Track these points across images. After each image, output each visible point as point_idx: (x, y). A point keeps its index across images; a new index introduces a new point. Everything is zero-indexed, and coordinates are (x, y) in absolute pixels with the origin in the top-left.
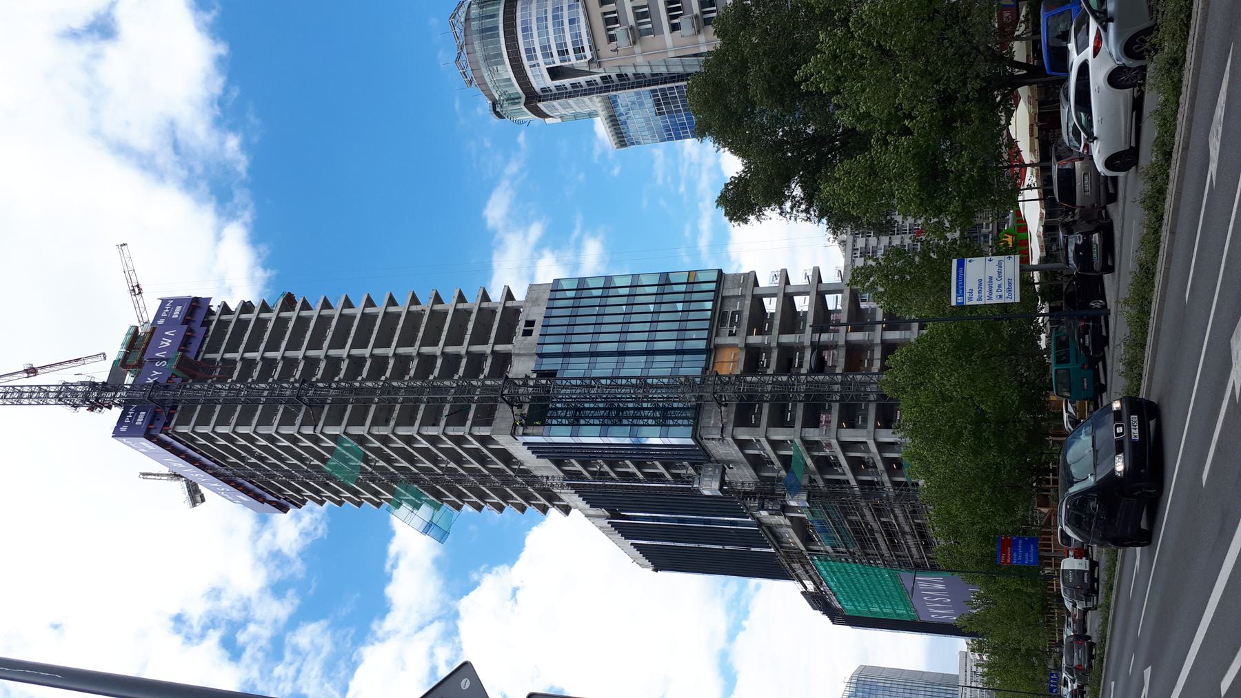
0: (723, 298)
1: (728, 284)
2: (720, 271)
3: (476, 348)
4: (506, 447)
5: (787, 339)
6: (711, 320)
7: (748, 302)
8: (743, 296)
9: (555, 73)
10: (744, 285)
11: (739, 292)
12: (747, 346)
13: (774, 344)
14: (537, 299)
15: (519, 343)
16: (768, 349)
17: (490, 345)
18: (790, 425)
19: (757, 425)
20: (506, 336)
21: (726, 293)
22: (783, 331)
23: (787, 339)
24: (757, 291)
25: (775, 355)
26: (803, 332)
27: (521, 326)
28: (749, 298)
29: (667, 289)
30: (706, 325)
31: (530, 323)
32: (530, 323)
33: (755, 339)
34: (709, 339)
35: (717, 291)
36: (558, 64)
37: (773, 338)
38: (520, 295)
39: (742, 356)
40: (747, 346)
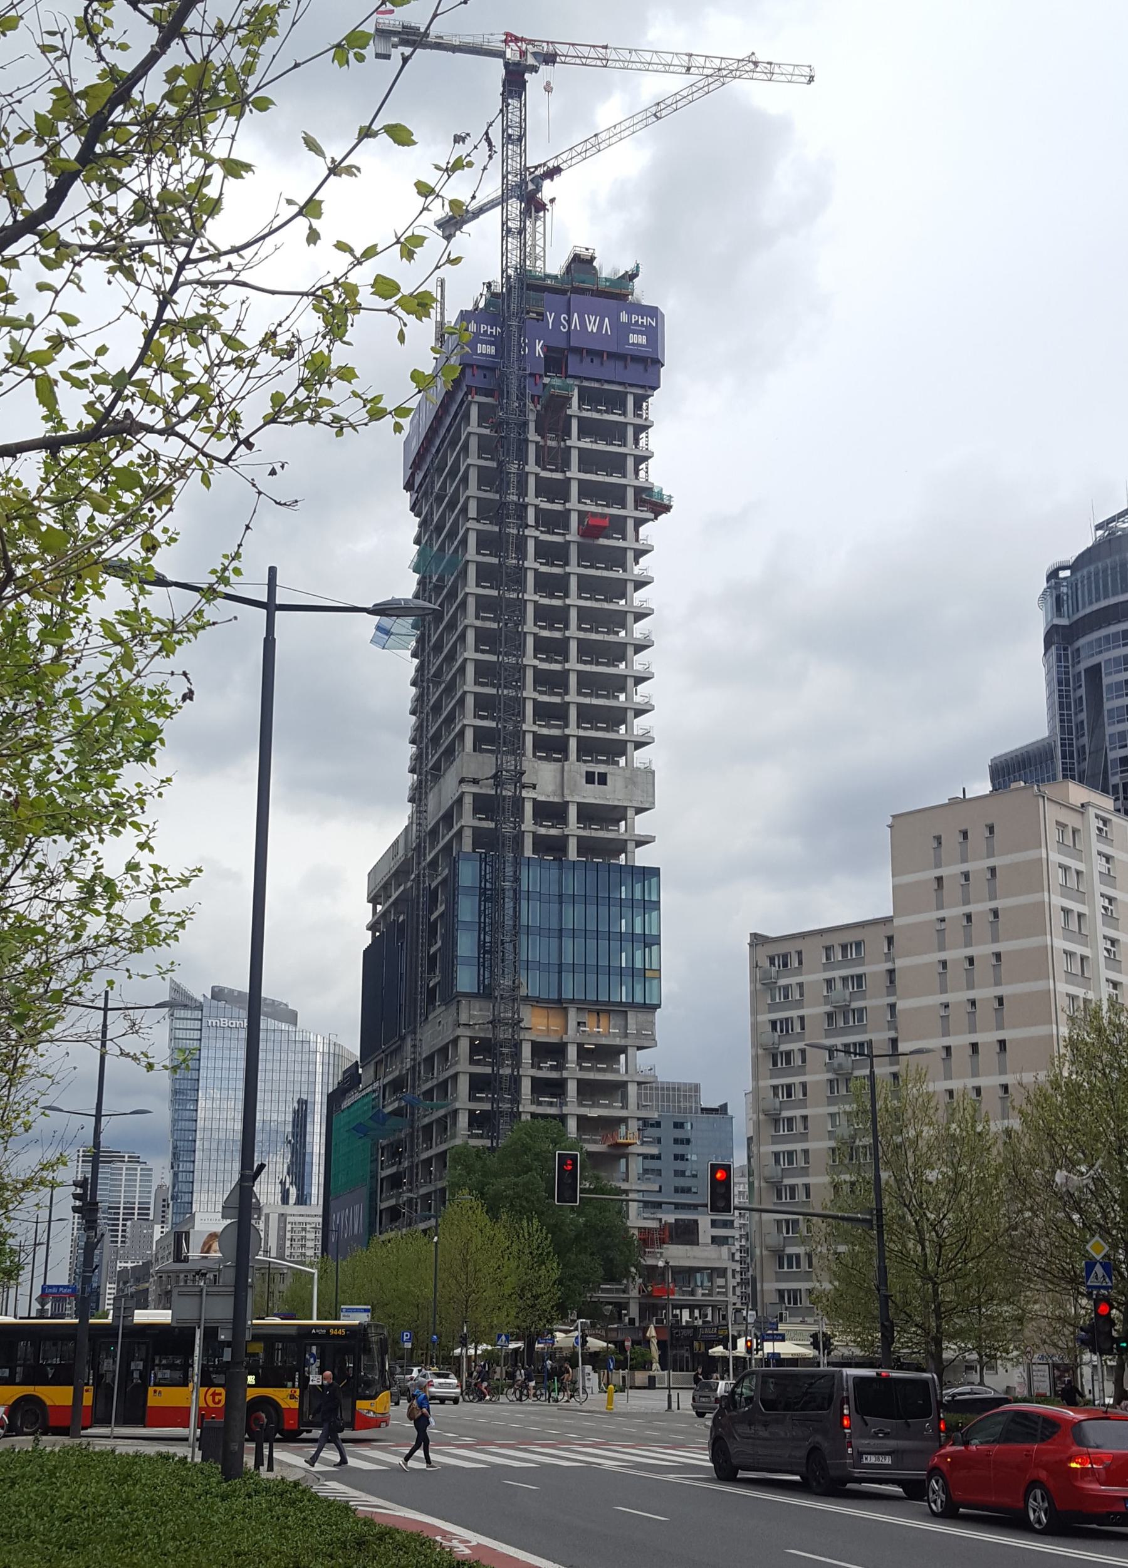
1: (642, 1017)
2: (659, 1006)
4: (457, 760)
5: (572, 1088)
7: (618, 1041)
8: (626, 1035)
9: (1095, 673)
10: (639, 1034)
11: (632, 1030)
13: (565, 1074)
14: (634, 783)
15: (576, 768)
16: (560, 1067)
18: (472, 1098)
19: (472, 1062)
20: (588, 748)
21: (631, 1016)
23: (572, 1088)
24: (630, 1051)
25: (554, 1075)
26: (580, 1104)
28: (623, 1042)
31: (603, 779)
32: (603, 779)
33: (572, 1052)
34: (573, 1001)
35: (633, 1005)
36: (1106, 681)
37: (573, 1071)
38: (640, 757)
39: (553, 1039)
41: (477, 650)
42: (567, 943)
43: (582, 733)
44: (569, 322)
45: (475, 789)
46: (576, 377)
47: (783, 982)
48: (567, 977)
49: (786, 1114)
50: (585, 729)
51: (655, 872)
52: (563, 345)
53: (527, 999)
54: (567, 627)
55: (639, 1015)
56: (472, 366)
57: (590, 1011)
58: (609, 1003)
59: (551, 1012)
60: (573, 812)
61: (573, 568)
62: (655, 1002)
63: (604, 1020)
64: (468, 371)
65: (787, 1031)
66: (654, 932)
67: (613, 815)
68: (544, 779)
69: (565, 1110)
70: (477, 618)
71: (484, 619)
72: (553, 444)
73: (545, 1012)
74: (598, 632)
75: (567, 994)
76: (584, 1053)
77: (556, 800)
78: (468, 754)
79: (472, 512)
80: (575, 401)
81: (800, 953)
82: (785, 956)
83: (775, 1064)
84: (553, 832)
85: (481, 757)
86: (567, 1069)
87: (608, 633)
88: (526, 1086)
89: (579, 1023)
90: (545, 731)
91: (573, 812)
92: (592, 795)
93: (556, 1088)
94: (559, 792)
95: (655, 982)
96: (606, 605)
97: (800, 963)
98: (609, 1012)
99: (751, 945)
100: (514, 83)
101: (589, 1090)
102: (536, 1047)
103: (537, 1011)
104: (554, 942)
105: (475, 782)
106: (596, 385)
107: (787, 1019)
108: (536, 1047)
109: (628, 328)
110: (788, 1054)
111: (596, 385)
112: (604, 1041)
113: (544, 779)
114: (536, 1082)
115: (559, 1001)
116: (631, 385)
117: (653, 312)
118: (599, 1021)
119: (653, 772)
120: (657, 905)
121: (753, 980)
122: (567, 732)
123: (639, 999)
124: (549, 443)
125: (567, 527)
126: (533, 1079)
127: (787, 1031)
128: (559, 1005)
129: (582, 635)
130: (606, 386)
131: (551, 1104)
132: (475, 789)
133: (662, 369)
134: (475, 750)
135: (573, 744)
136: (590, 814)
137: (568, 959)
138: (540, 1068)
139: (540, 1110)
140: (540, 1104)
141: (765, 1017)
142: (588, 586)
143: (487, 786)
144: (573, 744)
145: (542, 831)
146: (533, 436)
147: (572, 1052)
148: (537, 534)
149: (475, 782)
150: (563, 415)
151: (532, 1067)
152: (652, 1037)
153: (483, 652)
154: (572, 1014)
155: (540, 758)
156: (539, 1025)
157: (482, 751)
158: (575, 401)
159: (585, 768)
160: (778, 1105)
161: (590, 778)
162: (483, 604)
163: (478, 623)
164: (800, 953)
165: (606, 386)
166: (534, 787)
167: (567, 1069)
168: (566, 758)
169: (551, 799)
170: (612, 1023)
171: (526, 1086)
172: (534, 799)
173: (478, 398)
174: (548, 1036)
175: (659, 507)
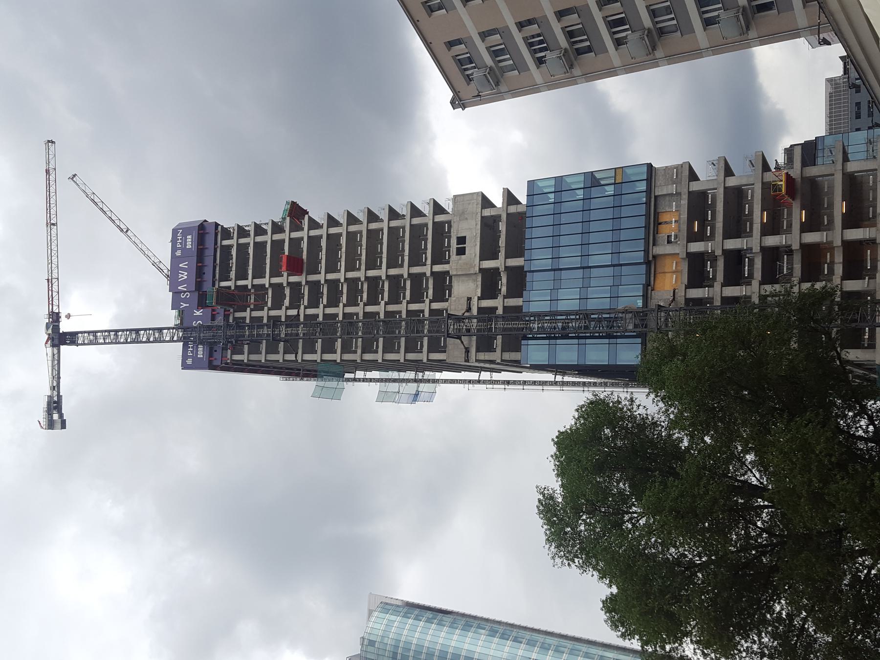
0: (656, 197)
1: (660, 180)
2: (650, 166)
3: (416, 270)
5: (732, 244)
6: (647, 227)
8: (678, 194)
10: (678, 182)
11: (673, 189)
12: (689, 255)
14: (463, 213)
15: (454, 265)
17: (429, 267)
20: (439, 257)
21: (659, 192)
22: (727, 236)
23: (732, 244)
25: (721, 264)
27: (454, 242)
29: (595, 192)
30: (641, 233)
31: (462, 240)
32: (462, 240)
33: (696, 247)
34: (646, 251)
35: (649, 191)
37: (716, 245)
39: (685, 267)
40: (689, 255)
41: (376, 352)
42: (593, 261)
43: (429, 262)
44: (185, 292)
45: (473, 350)
46: (214, 285)
47: (488, 60)
48: (624, 259)
49: (647, 22)
50: (426, 259)
51: (531, 184)
52: (197, 294)
53: (646, 297)
54: (359, 279)
55: (658, 183)
56: (210, 362)
57: (656, 232)
58: (647, 215)
59: (659, 270)
60: (488, 264)
61: (321, 277)
62: (645, 169)
63: (664, 218)
64: (216, 363)
65: (541, 42)
66: (582, 178)
67: (489, 225)
68: (465, 291)
69: (756, 249)
70: (355, 352)
71: (356, 347)
72: (253, 297)
73: (659, 276)
74: (361, 255)
75: (640, 257)
76: (700, 237)
77: (480, 279)
78: (448, 357)
79: (291, 357)
80: (224, 284)
81: (451, 44)
82: (460, 63)
83: (589, 50)
84: (504, 280)
85: (450, 347)
86: (713, 252)
87: (361, 246)
88: (732, 291)
89: (669, 242)
90: (431, 292)
91: (488, 264)
92: (473, 248)
93: (735, 259)
94: (474, 277)
95: (629, 171)
96: (344, 249)
97: (459, 42)
98: (657, 214)
99: (464, 107)
100: (71, 338)
101: (736, 226)
102: (691, 285)
103: (659, 284)
104: (595, 272)
105: (467, 351)
106: (218, 269)
107: (530, 45)
108: (691, 285)
109: (184, 249)
110: (570, 35)
111: (218, 269)
112: (684, 216)
113: (465, 291)
114: (729, 281)
115: (648, 263)
116: (216, 243)
117: (175, 232)
118: (666, 223)
119: (455, 197)
120: (559, 180)
121: (499, 96)
122: (428, 274)
123: (643, 186)
124: (252, 301)
125: (299, 284)
126: (724, 285)
127: (541, 42)
128: (651, 263)
129: (363, 267)
130: (218, 261)
131: (751, 262)
132: (473, 350)
133: (210, 221)
134: (445, 352)
135: (438, 268)
136: (489, 251)
137: (607, 260)
138: (714, 278)
139: (758, 275)
140: (751, 275)
141: (536, 73)
142: (332, 267)
143: (470, 341)
144: (438, 268)
145: (504, 290)
146: (247, 314)
147: (696, 247)
148: (302, 307)
149: (467, 351)
150: (236, 292)
151: (712, 286)
152: (679, 168)
153: (377, 347)
154: (658, 250)
155: (450, 295)
156: (671, 283)
157: (445, 346)
158: (224, 284)
159: (454, 257)
160: (637, 35)
161: (461, 252)
162: (346, 349)
163: (359, 351)
164: (451, 44)
165: (218, 261)
166: (469, 299)
167: (713, 252)
168: (447, 273)
169: (480, 283)
170: (668, 209)
171: (732, 291)
172: (479, 299)
173: (229, 357)
174: (681, 272)
175: (296, 212)
